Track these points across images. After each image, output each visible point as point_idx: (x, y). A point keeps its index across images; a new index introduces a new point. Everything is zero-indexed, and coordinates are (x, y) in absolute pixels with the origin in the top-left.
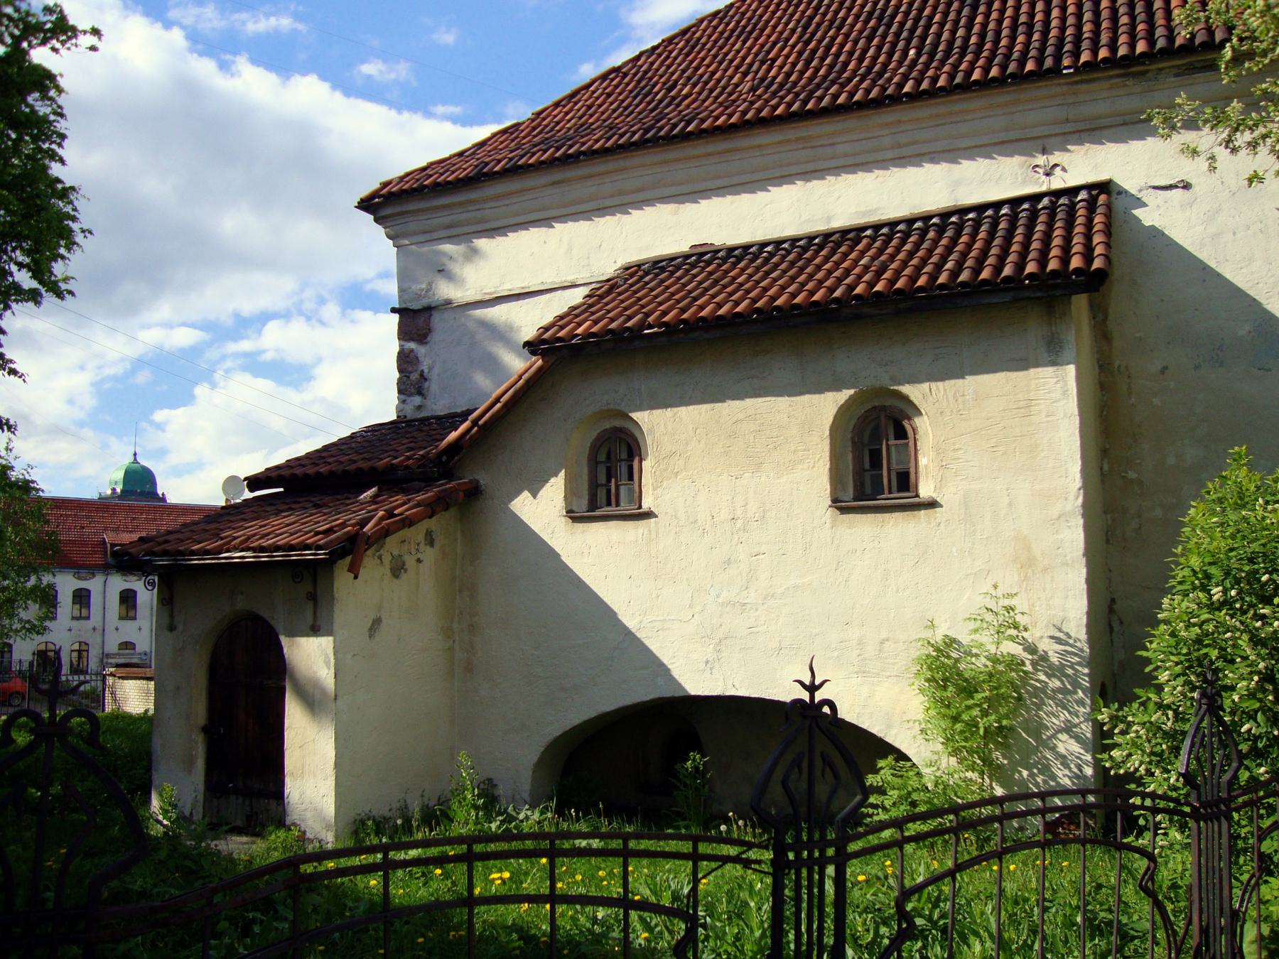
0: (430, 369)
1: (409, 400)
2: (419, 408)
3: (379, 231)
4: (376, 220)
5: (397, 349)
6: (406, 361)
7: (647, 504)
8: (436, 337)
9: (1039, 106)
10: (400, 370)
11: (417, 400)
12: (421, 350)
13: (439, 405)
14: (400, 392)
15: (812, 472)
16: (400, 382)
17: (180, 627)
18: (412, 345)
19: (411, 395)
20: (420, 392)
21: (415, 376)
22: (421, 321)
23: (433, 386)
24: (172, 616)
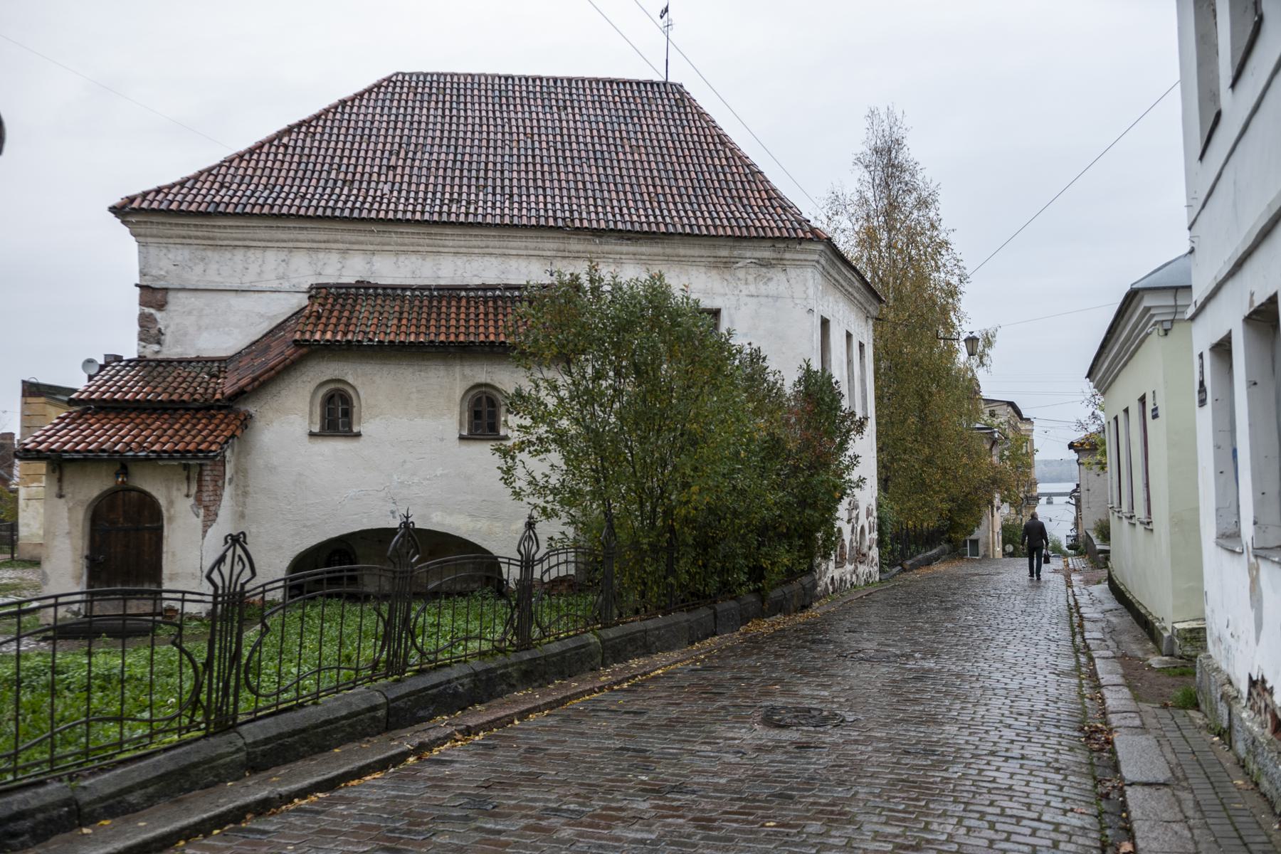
0: (166, 327)
2: (157, 352)
3: (126, 230)
4: (123, 222)
5: (138, 313)
6: (146, 323)
7: (355, 429)
8: (170, 307)
9: (550, 245)
10: (141, 326)
11: (156, 347)
12: (158, 315)
13: (171, 350)
14: (141, 340)
15: (451, 422)
16: (140, 333)
18: (147, 310)
19: (151, 343)
20: (159, 343)
21: (154, 331)
22: (159, 296)
23: (168, 339)
24: (60, 488)
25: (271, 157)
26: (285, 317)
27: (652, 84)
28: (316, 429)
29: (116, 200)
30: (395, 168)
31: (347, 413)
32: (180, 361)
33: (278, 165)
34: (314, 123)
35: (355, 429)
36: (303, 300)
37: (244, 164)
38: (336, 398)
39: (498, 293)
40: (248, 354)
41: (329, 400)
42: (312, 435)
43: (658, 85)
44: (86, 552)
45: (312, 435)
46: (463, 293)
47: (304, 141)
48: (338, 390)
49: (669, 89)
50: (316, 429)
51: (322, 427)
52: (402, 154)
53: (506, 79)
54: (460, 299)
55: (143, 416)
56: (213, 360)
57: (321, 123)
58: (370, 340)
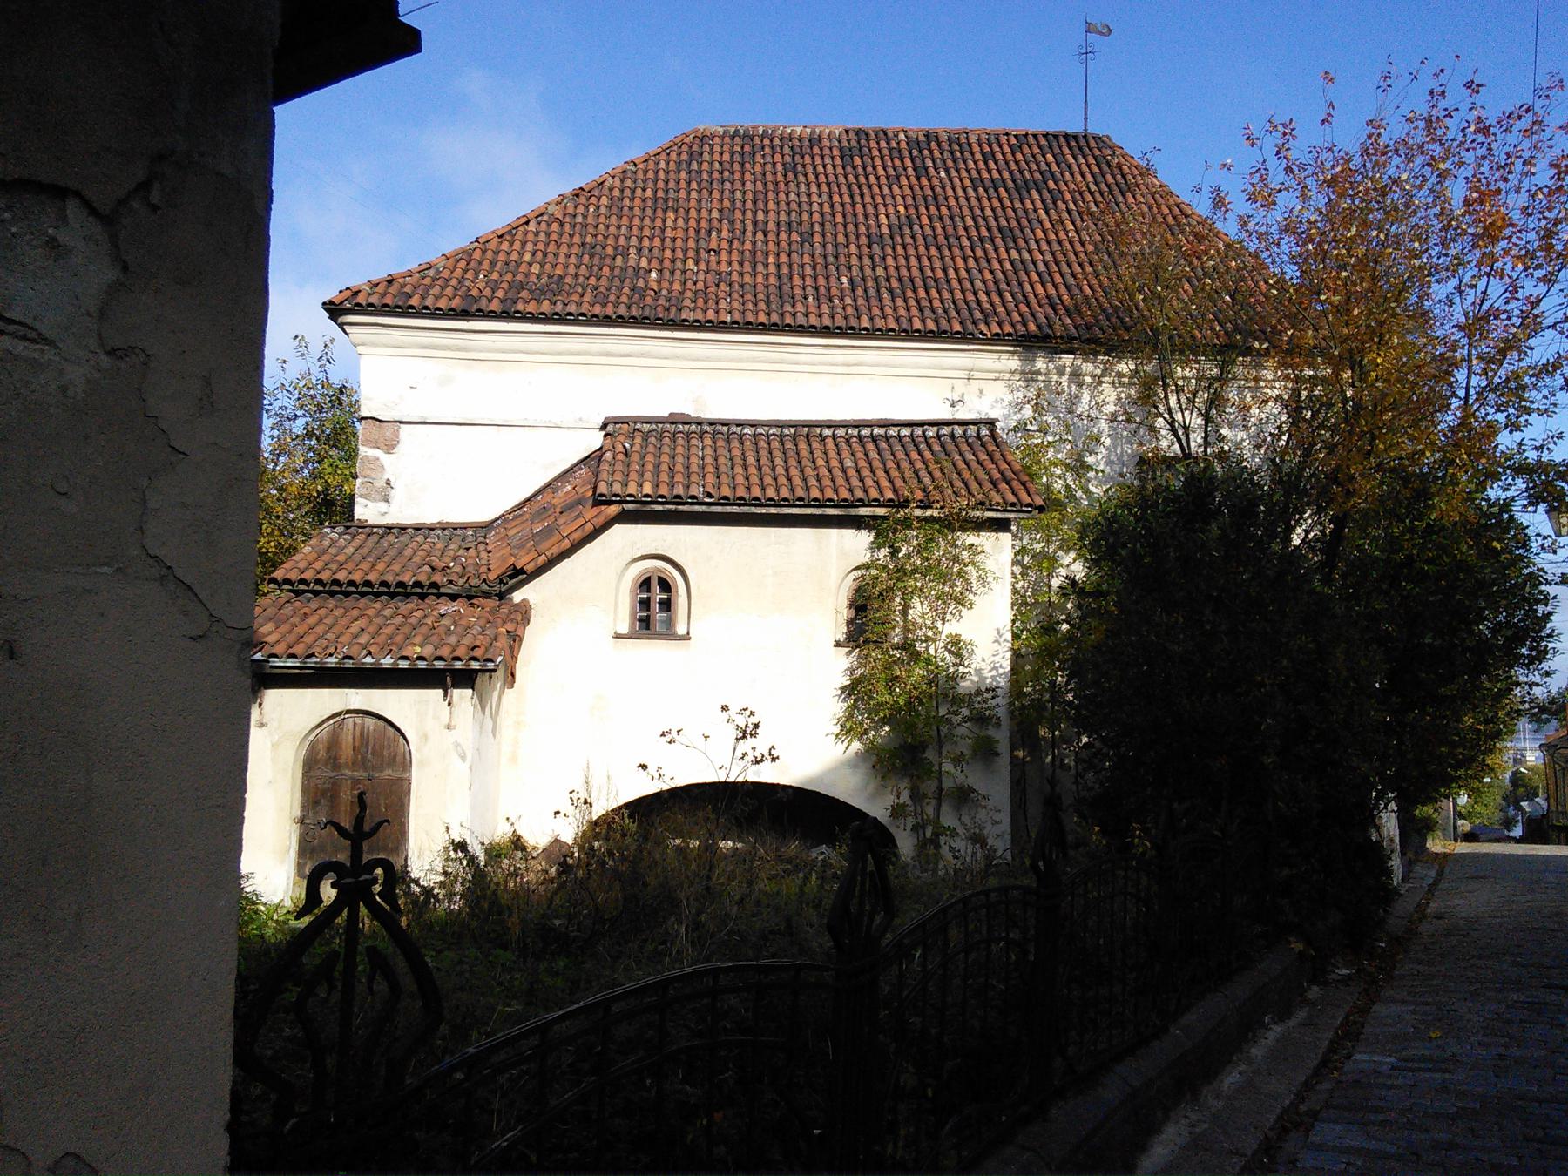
1: (371, 505)
11: (383, 506)
17: (273, 725)
19: (375, 500)
21: (380, 484)
22: (388, 431)
23: (396, 495)
25: (542, 237)
26: (567, 466)
27: (1066, 136)
28: (624, 628)
29: (331, 294)
30: (718, 252)
31: (667, 605)
32: (417, 528)
33: (552, 248)
34: (595, 193)
35: (681, 629)
36: (596, 440)
37: (505, 246)
38: (654, 582)
39: (876, 431)
40: (516, 517)
41: (645, 584)
42: (618, 636)
43: (1075, 137)
44: (297, 813)
45: (618, 636)
46: (827, 432)
47: (585, 217)
48: (659, 570)
49: (1093, 144)
50: (624, 630)
51: (632, 624)
52: (725, 234)
53: (857, 132)
54: (823, 439)
55: (378, 605)
56: (464, 527)
57: (606, 191)
58: (710, 495)
